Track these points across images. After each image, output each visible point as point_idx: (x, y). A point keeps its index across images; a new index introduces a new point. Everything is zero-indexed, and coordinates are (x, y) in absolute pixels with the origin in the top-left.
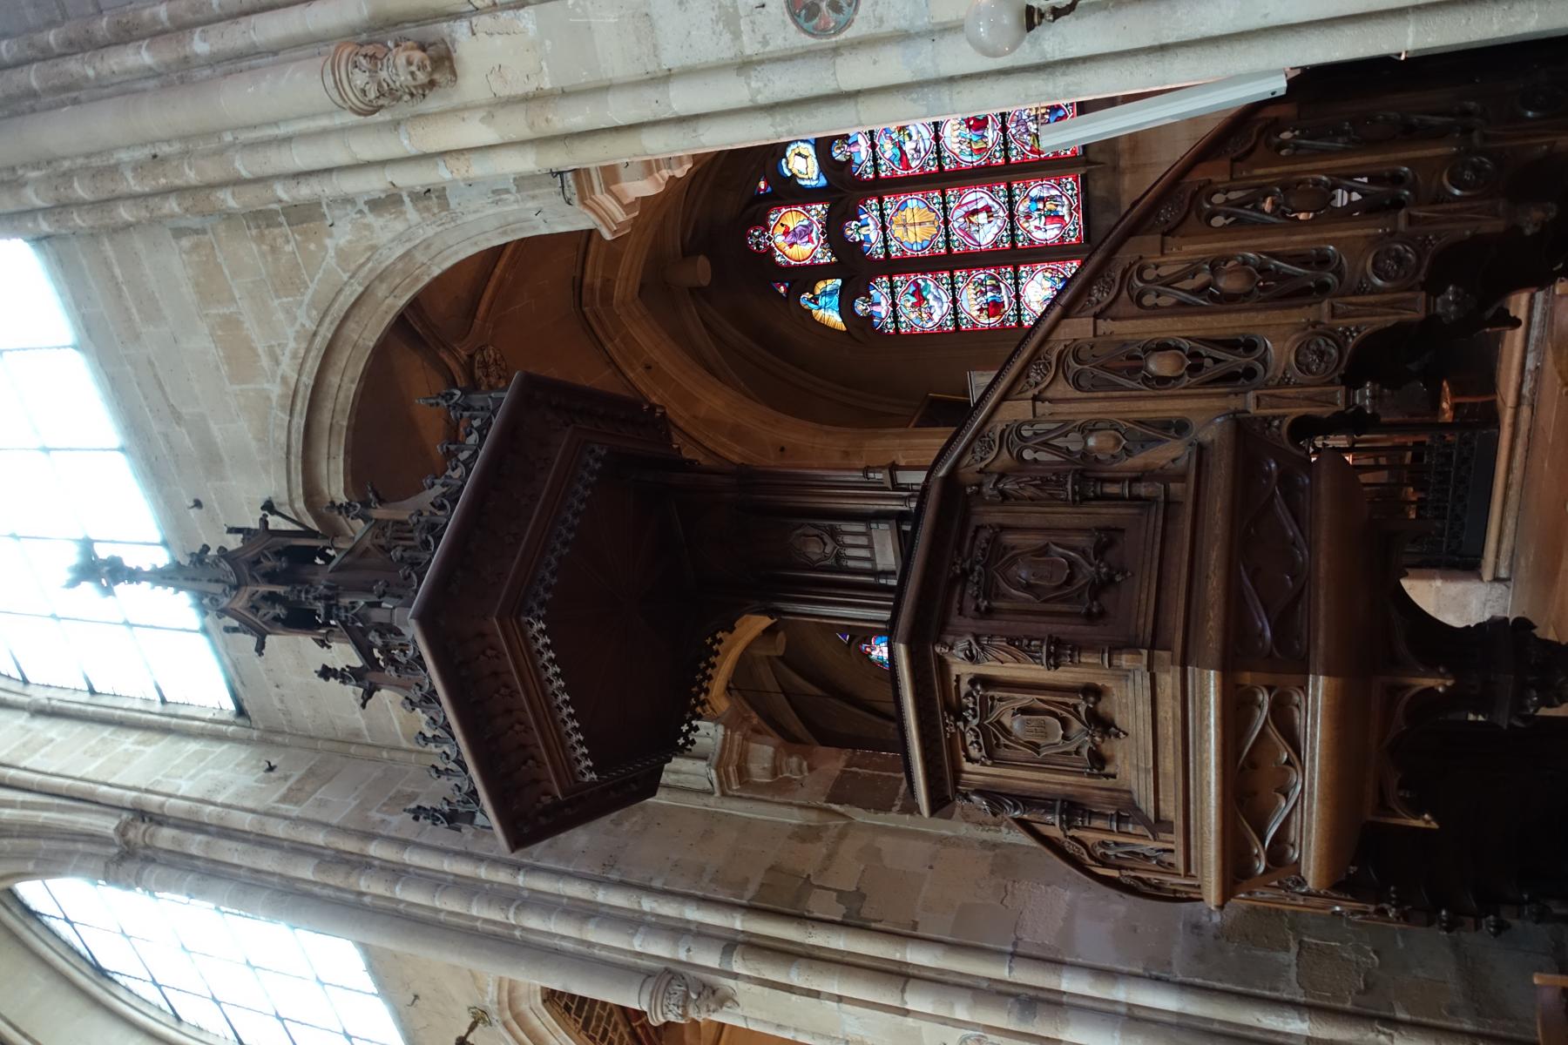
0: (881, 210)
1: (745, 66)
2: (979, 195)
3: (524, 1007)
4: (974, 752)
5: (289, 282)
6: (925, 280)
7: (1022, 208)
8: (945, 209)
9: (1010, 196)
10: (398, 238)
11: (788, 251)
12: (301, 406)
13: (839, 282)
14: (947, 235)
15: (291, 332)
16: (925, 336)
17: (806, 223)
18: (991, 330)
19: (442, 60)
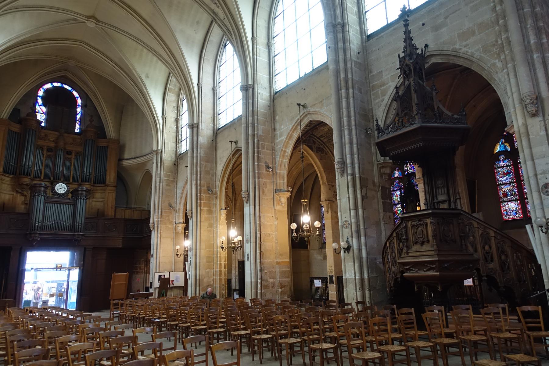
1: (536, 175)
3: (309, 116)
4: (413, 223)
5: (485, 50)
10: (500, 79)
12: (454, 53)
13: (509, 150)
15: (473, 50)
16: (495, 177)
18: (499, 195)
19: (534, 115)
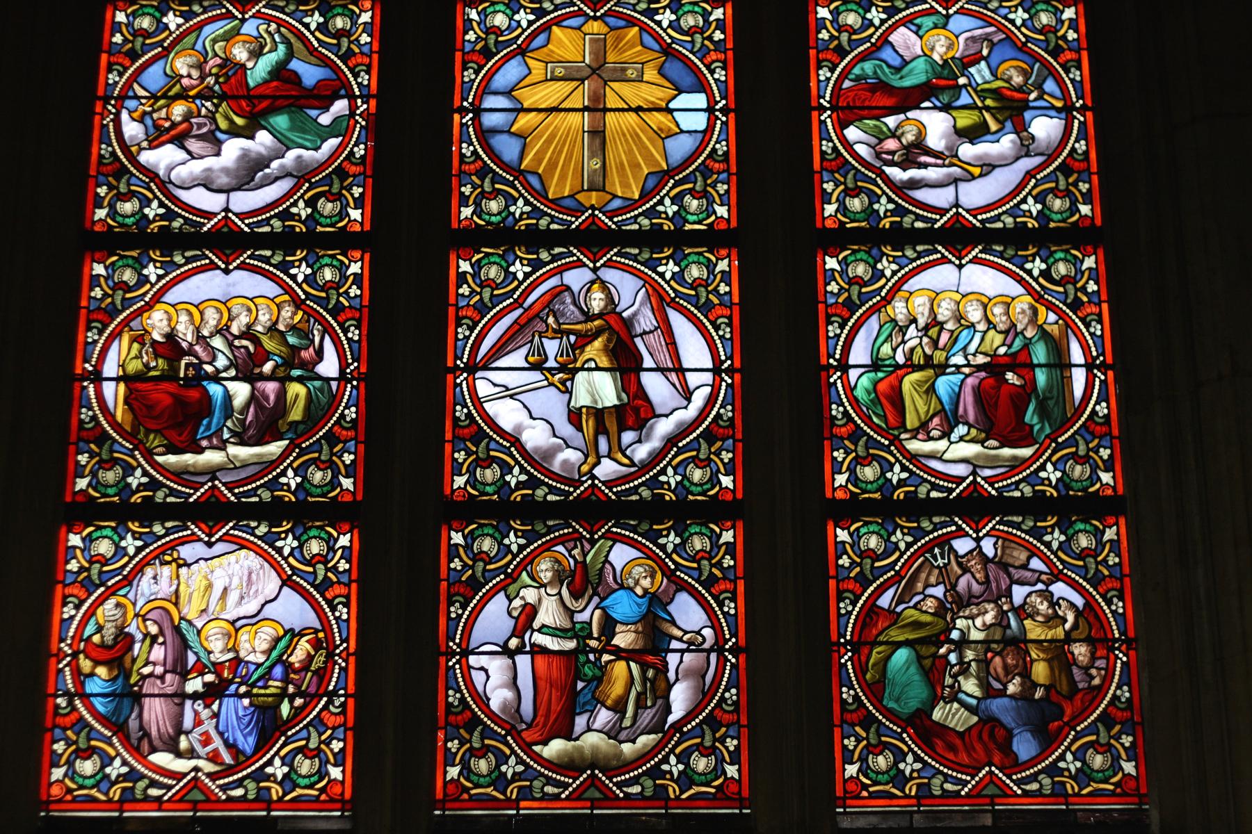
6: (340, 128)
7: (621, 555)
8: (654, 240)
9: (686, 512)
14: (535, 239)
18: (64, 377)
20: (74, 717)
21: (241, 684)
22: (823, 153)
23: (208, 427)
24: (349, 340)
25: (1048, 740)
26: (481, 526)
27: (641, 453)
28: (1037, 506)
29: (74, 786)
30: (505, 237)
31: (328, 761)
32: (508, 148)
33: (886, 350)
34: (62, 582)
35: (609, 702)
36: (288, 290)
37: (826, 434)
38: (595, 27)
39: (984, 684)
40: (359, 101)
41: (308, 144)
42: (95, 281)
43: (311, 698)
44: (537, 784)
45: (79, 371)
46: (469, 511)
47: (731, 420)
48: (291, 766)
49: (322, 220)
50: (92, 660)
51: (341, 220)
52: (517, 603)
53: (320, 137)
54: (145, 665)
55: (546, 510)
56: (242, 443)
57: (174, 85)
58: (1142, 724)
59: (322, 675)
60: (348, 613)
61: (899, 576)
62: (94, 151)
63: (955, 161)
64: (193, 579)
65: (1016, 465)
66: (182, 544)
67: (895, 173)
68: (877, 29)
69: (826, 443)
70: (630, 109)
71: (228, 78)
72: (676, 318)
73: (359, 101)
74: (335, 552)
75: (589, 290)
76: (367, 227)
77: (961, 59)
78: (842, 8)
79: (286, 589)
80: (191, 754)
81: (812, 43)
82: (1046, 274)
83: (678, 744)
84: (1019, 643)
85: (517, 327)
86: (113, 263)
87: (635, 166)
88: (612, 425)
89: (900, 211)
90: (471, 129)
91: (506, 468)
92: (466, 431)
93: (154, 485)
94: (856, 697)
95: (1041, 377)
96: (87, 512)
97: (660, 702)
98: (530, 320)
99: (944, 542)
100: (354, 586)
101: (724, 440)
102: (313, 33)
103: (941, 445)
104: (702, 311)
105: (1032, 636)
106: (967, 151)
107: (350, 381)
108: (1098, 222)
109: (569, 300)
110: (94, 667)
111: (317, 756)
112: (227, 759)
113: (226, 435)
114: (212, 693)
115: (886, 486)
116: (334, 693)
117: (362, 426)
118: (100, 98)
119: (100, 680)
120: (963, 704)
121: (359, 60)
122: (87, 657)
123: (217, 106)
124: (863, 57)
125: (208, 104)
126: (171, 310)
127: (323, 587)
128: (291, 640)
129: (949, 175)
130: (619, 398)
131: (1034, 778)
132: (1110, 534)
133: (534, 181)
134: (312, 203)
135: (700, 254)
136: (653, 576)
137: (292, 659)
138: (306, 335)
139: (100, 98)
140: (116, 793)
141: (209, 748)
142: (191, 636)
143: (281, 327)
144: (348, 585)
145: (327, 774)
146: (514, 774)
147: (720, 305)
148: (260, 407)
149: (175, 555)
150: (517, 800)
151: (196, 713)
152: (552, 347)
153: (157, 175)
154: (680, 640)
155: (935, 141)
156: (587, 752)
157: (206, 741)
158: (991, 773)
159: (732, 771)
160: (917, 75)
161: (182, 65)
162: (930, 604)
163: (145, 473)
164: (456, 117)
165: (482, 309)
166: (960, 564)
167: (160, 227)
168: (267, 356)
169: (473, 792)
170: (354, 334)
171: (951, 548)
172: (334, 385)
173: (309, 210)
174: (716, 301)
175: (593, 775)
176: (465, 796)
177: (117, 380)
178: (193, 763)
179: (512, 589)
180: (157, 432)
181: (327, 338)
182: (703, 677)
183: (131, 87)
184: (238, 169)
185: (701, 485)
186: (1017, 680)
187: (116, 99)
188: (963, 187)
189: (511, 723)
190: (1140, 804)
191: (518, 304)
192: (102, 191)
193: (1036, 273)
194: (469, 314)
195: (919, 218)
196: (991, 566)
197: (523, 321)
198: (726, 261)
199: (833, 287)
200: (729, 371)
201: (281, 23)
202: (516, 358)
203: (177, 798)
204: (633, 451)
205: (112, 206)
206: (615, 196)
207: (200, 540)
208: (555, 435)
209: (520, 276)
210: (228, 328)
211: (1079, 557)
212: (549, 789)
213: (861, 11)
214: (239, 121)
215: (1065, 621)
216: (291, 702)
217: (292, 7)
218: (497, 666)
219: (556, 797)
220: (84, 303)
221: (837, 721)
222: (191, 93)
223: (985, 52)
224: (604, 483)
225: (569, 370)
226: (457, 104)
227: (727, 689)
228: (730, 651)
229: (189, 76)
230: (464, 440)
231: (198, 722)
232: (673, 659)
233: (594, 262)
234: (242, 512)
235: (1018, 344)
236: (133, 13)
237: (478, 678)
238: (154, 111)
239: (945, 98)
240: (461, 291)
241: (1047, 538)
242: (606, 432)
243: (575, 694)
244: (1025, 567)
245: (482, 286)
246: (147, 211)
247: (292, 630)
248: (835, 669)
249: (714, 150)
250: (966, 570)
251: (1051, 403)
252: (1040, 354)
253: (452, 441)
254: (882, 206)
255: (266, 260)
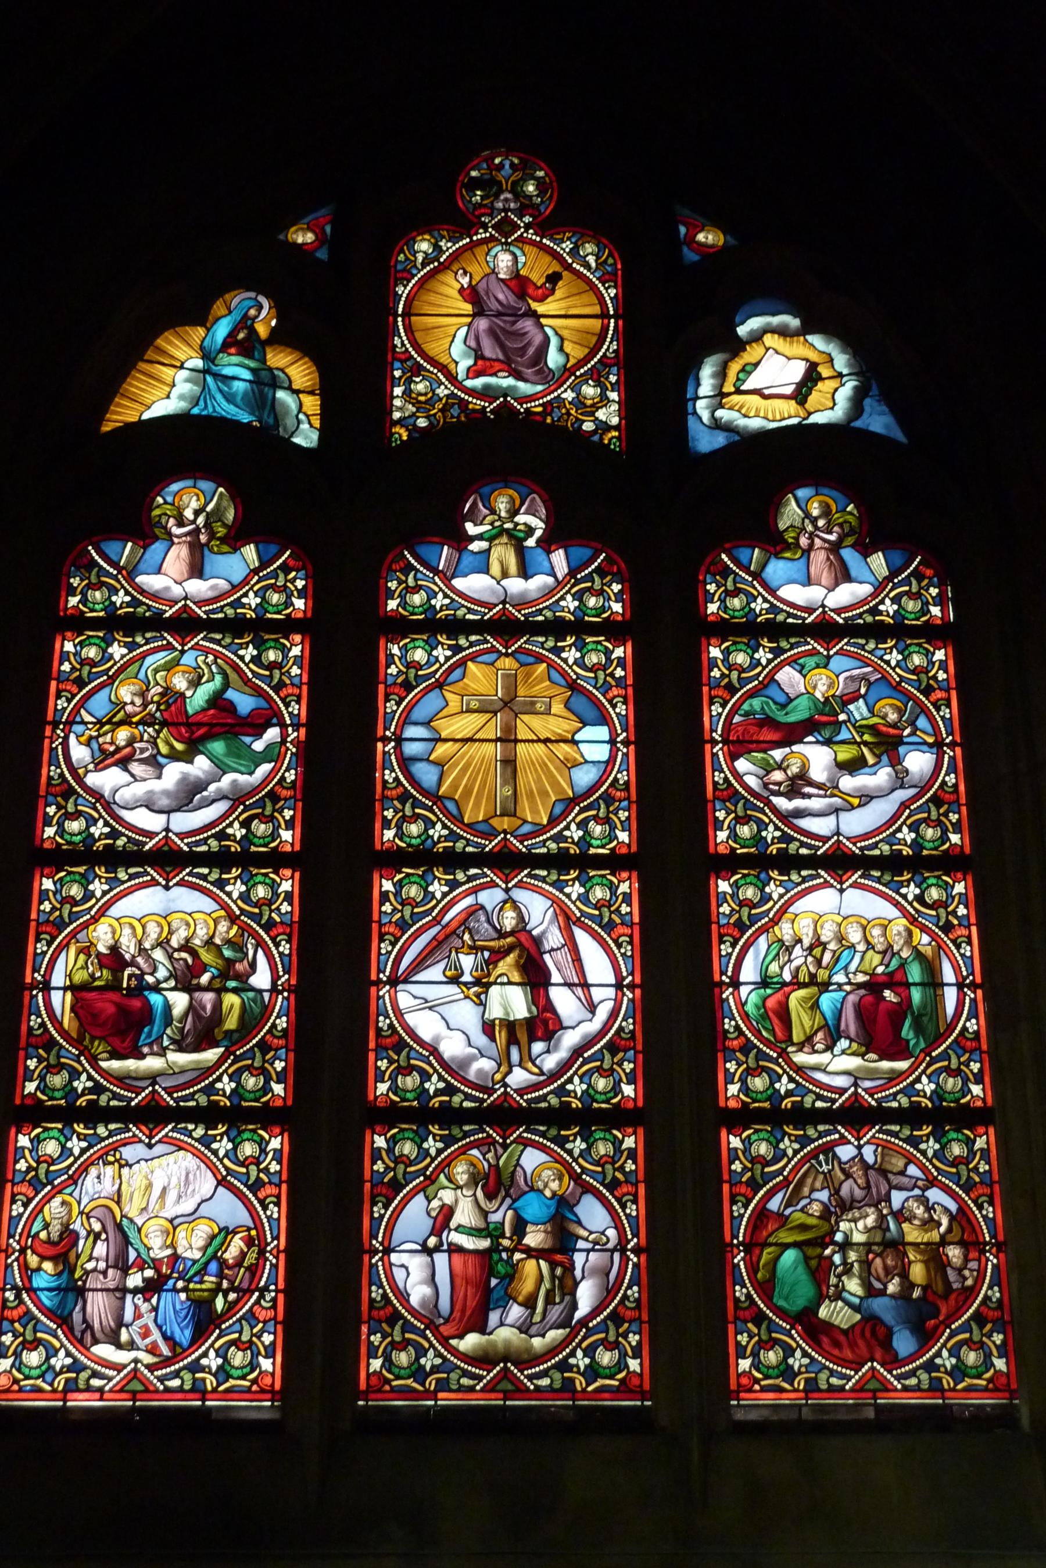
0: (578, 628)
2: (604, 996)
7: (532, 1159)
9: (589, 1118)
11: (452, 285)
13: (307, 437)
17: (554, 359)
20: (21, 1310)
21: (178, 1279)
22: (715, 784)
23: (149, 1035)
24: (281, 954)
25: (926, 1337)
26: (402, 1130)
27: (550, 1063)
28: (913, 1116)
29: (21, 1377)
30: (424, 858)
31: (259, 1353)
32: (426, 774)
33: (774, 968)
34: (12, 1181)
35: (520, 1299)
36: (224, 906)
37: (719, 1046)
38: (507, 662)
39: (867, 1285)
40: (290, 729)
41: (243, 769)
42: (44, 895)
43: (245, 1292)
44: (454, 1376)
45: (28, 980)
46: (389, 1116)
47: (632, 1032)
48: (225, 1358)
49: (256, 840)
50: (38, 1255)
51: (273, 840)
52: (435, 1204)
53: (254, 762)
54: (89, 1260)
55: (460, 1116)
56: (181, 1049)
57: (119, 711)
58: (1011, 1322)
59: (254, 1271)
60: (279, 1212)
61: (786, 1182)
62: (44, 771)
63: (836, 792)
64: (134, 1178)
65: (894, 1077)
66: (125, 1145)
67: (782, 803)
68: (764, 668)
69: (720, 1055)
70: (539, 740)
71: (169, 706)
72: (580, 935)
73: (290, 729)
74: (267, 1154)
75: (501, 909)
76: (297, 848)
77: (841, 697)
78: (732, 648)
79: (220, 1188)
80: (131, 1346)
81: (705, 680)
82: (920, 899)
83: (584, 1338)
84: (896, 1245)
85: (435, 943)
86: (61, 879)
87: (544, 794)
88: (522, 1036)
89: (786, 838)
90: (393, 757)
91: (425, 1076)
92: (388, 1040)
93: (98, 1089)
94: (749, 1296)
95: (916, 995)
96: (35, 1114)
97: (567, 1298)
98: (447, 937)
99: (828, 1149)
100: (284, 1187)
101: (625, 1051)
102: (247, 665)
103: (826, 1057)
104: (605, 928)
105: (909, 1238)
106: (847, 783)
107: (281, 992)
108: (967, 850)
109: (483, 918)
110: (41, 1263)
111: (250, 1348)
112: (166, 1351)
113: (166, 1043)
114: (151, 1288)
115: (775, 1097)
116: (266, 1288)
117: (292, 1034)
118: (49, 723)
119: (46, 1275)
120: (847, 1303)
121: (290, 691)
122: (34, 1252)
123: (158, 732)
124: (752, 694)
125: (150, 730)
126: (116, 924)
127: (256, 1187)
128: (226, 1238)
129: (831, 805)
130: (529, 1011)
131: (913, 1373)
132: (980, 1143)
133: (451, 806)
134: (246, 824)
135: (603, 876)
136: (560, 1178)
137: (226, 1256)
138: (239, 947)
139: (49, 723)
140: (60, 1383)
141: (148, 1341)
142: (132, 1234)
143: (218, 941)
144: (279, 1186)
145: (259, 1365)
146: (433, 1366)
147: (622, 924)
148: (198, 1016)
149: (118, 1156)
150: (436, 1392)
151: (136, 1307)
152: (467, 962)
153: (102, 796)
154: (586, 1240)
155: (819, 773)
156: (500, 1346)
157: (146, 1333)
158: (873, 1368)
159: (634, 1365)
160: (799, 713)
161: (126, 692)
162: (816, 1208)
163: (90, 1078)
164: (380, 745)
165: (403, 926)
166: (843, 1170)
167: (105, 845)
168: (204, 968)
169: (394, 1383)
170: (285, 948)
171: (835, 1155)
172: (266, 996)
173: (244, 831)
174: (618, 921)
175: (506, 1369)
176: (387, 1388)
177: (65, 989)
178: (134, 1354)
179: (430, 1190)
180: (101, 1038)
181: (260, 952)
182: (608, 1275)
183: (79, 712)
184: (177, 791)
185: (605, 1093)
186: (896, 1280)
187: (65, 724)
188: (843, 816)
189: (430, 1318)
190: (1011, 1398)
191: (436, 921)
192: (51, 810)
193: (910, 897)
194: (391, 930)
195: (803, 844)
196: (871, 1173)
197: (441, 937)
198: (627, 883)
199: (725, 909)
200: (632, 987)
201: (217, 656)
202: (435, 972)
203: (117, 1388)
204: (542, 1061)
205: (60, 825)
206: (525, 821)
207: (140, 1141)
208: (470, 1045)
209: (438, 895)
210: (168, 941)
211: (953, 1164)
212: (465, 1381)
213: (749, 651)
214: (179, 746)
215: (939, 1224)
216: (225, 1296)
217: (228, 640)
218: (417, 1264)
219: (472, 1389)
220: (34, 916)
221: (730, 1318)
222: (135, 720)
223: (863, 691)
224: (515, 1091)
225: (482, 983)
226: (380, 733)
227: (629, 1287)
228: (633, 1251)
229: (133, 703)
230: (386, 1049)
231: (138, 1315)
232: (579, 1258)
233: (507, 883)
234: (180, 1115)
235: (894, 963)
236: (80, 643)
237: (399, 1275)
238: (99, 736)
239: (827, 733)
240: (383, 909)
241: (923, 1146)
242: (517, 1043)
243: (488, 1291)
244: (902, 1173)
245: (403, 904)
246: (92, 830)
247: (226, 1228)
248: (729, 1268)
249: (616, 780)
250: (848, 1176)
251: (925, 1019)
252: (915, 973)
253: (375, 1050)
254: (770, 833)
255: (204, 877)
